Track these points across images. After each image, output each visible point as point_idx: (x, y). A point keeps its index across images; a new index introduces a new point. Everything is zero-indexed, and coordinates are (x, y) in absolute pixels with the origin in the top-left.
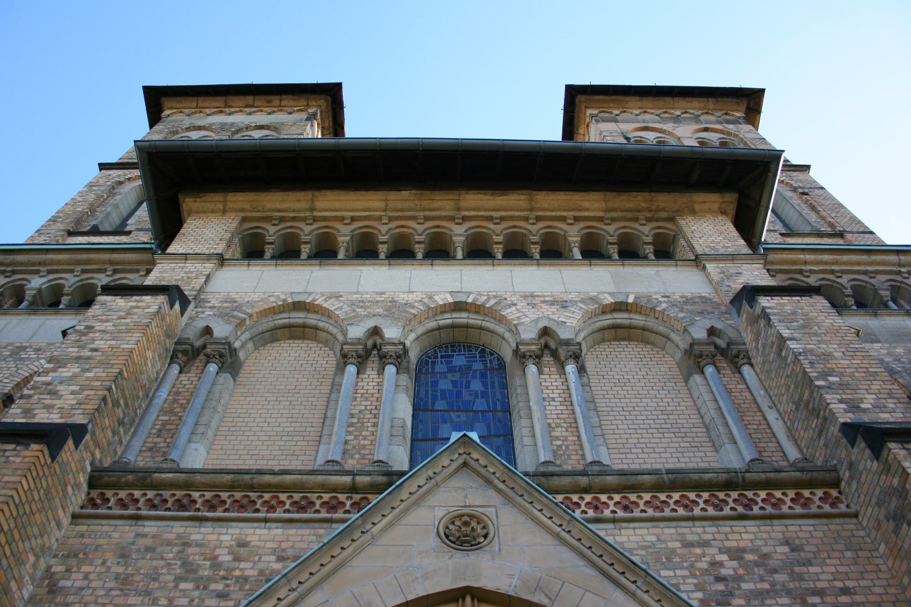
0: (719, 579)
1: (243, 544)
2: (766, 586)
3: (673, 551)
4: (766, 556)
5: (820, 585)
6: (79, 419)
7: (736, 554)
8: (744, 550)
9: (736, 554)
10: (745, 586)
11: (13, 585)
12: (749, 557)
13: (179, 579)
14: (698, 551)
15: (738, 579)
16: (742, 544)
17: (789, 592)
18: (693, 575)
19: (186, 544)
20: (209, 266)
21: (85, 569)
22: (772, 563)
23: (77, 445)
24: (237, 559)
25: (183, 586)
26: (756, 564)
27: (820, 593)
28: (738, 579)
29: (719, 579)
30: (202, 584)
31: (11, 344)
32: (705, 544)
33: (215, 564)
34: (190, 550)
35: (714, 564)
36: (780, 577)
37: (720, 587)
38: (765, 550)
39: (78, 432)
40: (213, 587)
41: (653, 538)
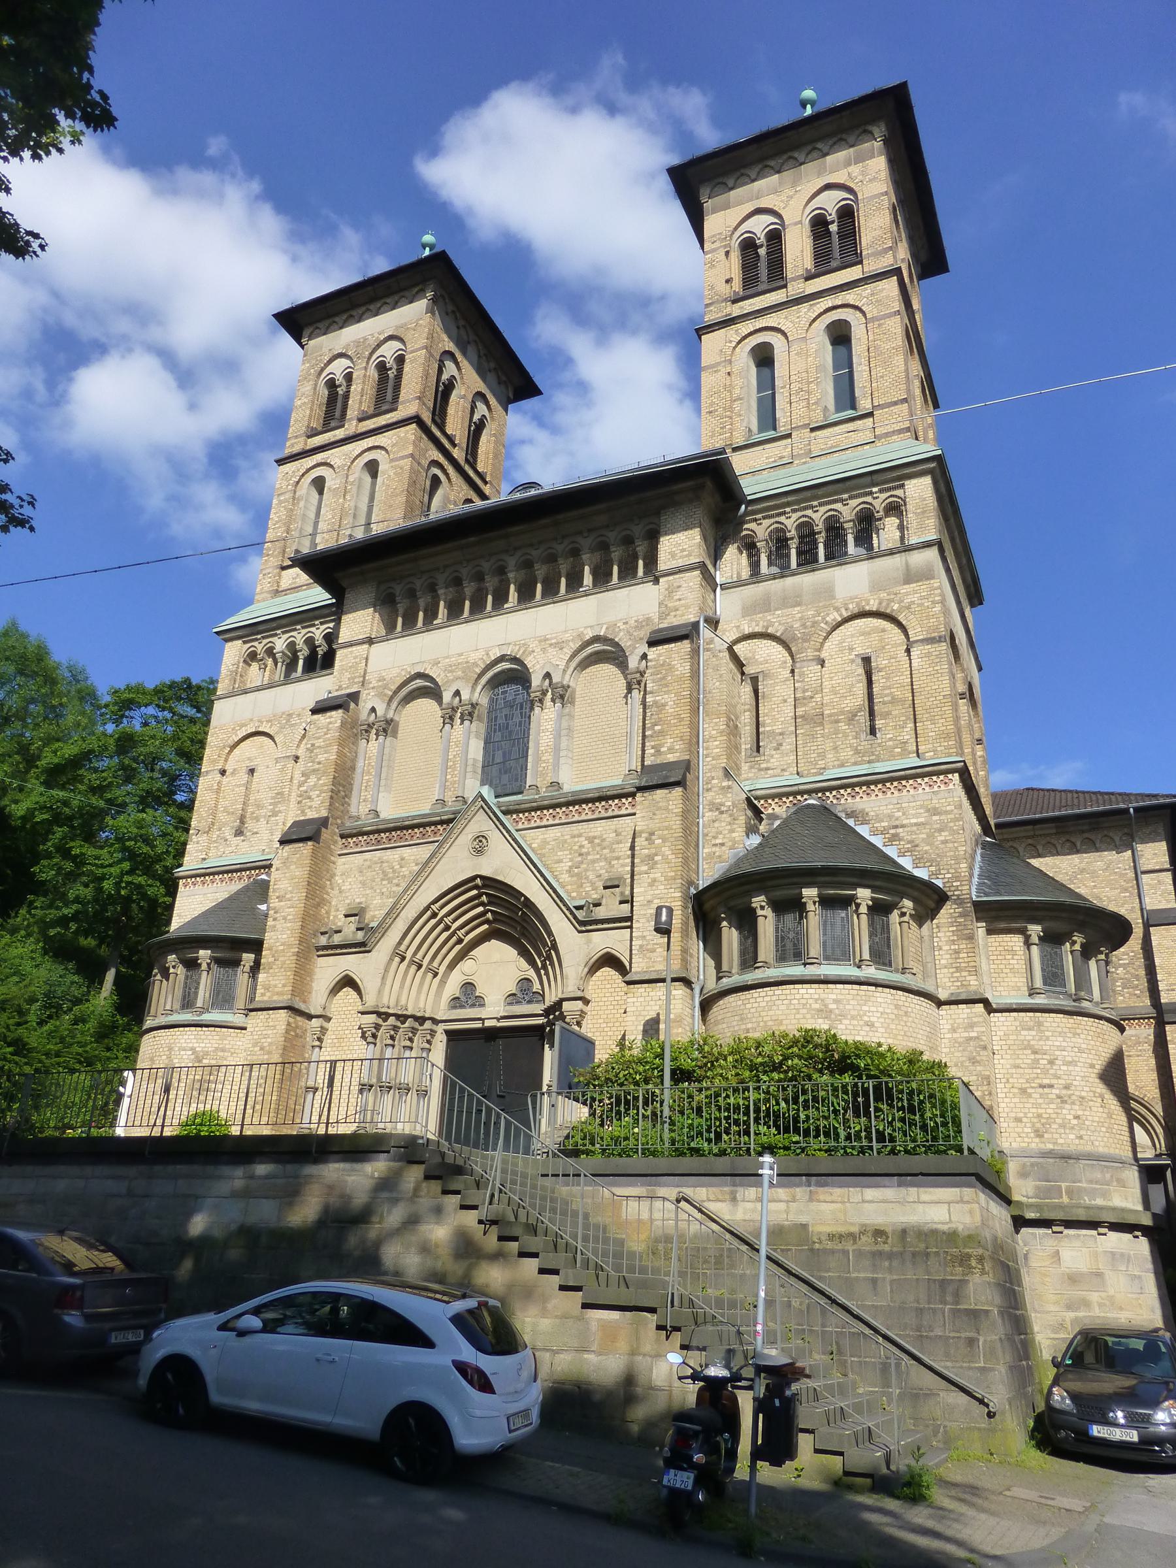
0: (581, 855)
1: (402, 859)
2: (598, 856)
3: (565, 841)
4: (603, 840)
5: (620, 854)
6: (324, 813)
7: (591, 840)
8: (595, 837)
9: (591, 840)
10: (589, 857)
11: (325, 896)
12: (597, 841)
13: (382, 880)
14: (576, 839)
15: (588, 854)
16: (596, 834)
17: (606, 859)
18: (570, 854)
19: (382, 862)
20: (366, 646)
21: (350, 880)
22: (605, 844)
23: (327, 828)
24: (401, 867)
25: (384, 882)
26: (599, 845)
27: (618, 858)
28: (588, 854)
29: (581, 855)
30: (390, 881)
31: (283, 713)
32: (580, 836)
33: (394, 872)
34: (385, 865)
35: (582, 846)
36: (606, 851)
37: (580, 859)
38: (604, 837)
39: (324, 822)
40: (394, 881)
41: (559, 834)
